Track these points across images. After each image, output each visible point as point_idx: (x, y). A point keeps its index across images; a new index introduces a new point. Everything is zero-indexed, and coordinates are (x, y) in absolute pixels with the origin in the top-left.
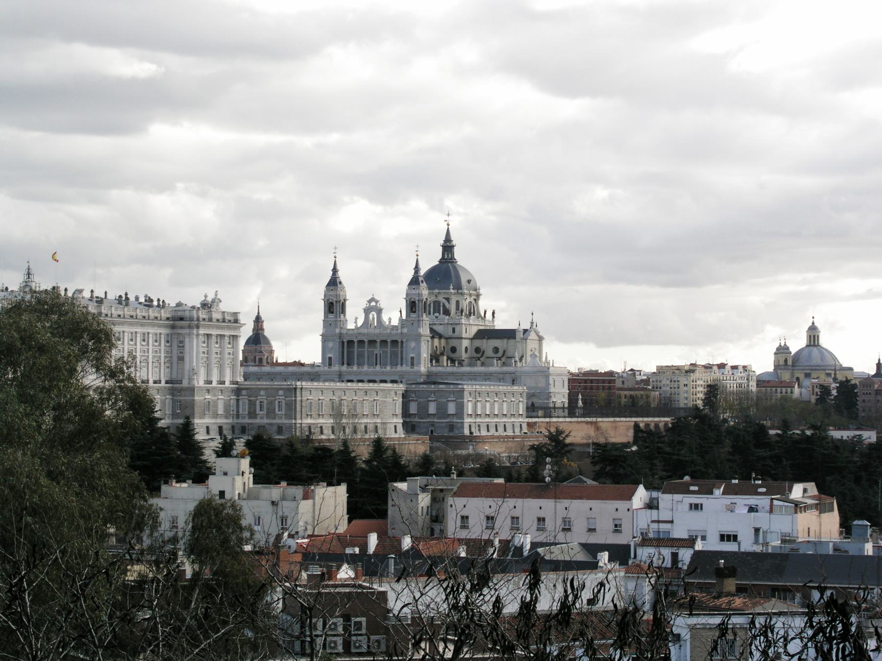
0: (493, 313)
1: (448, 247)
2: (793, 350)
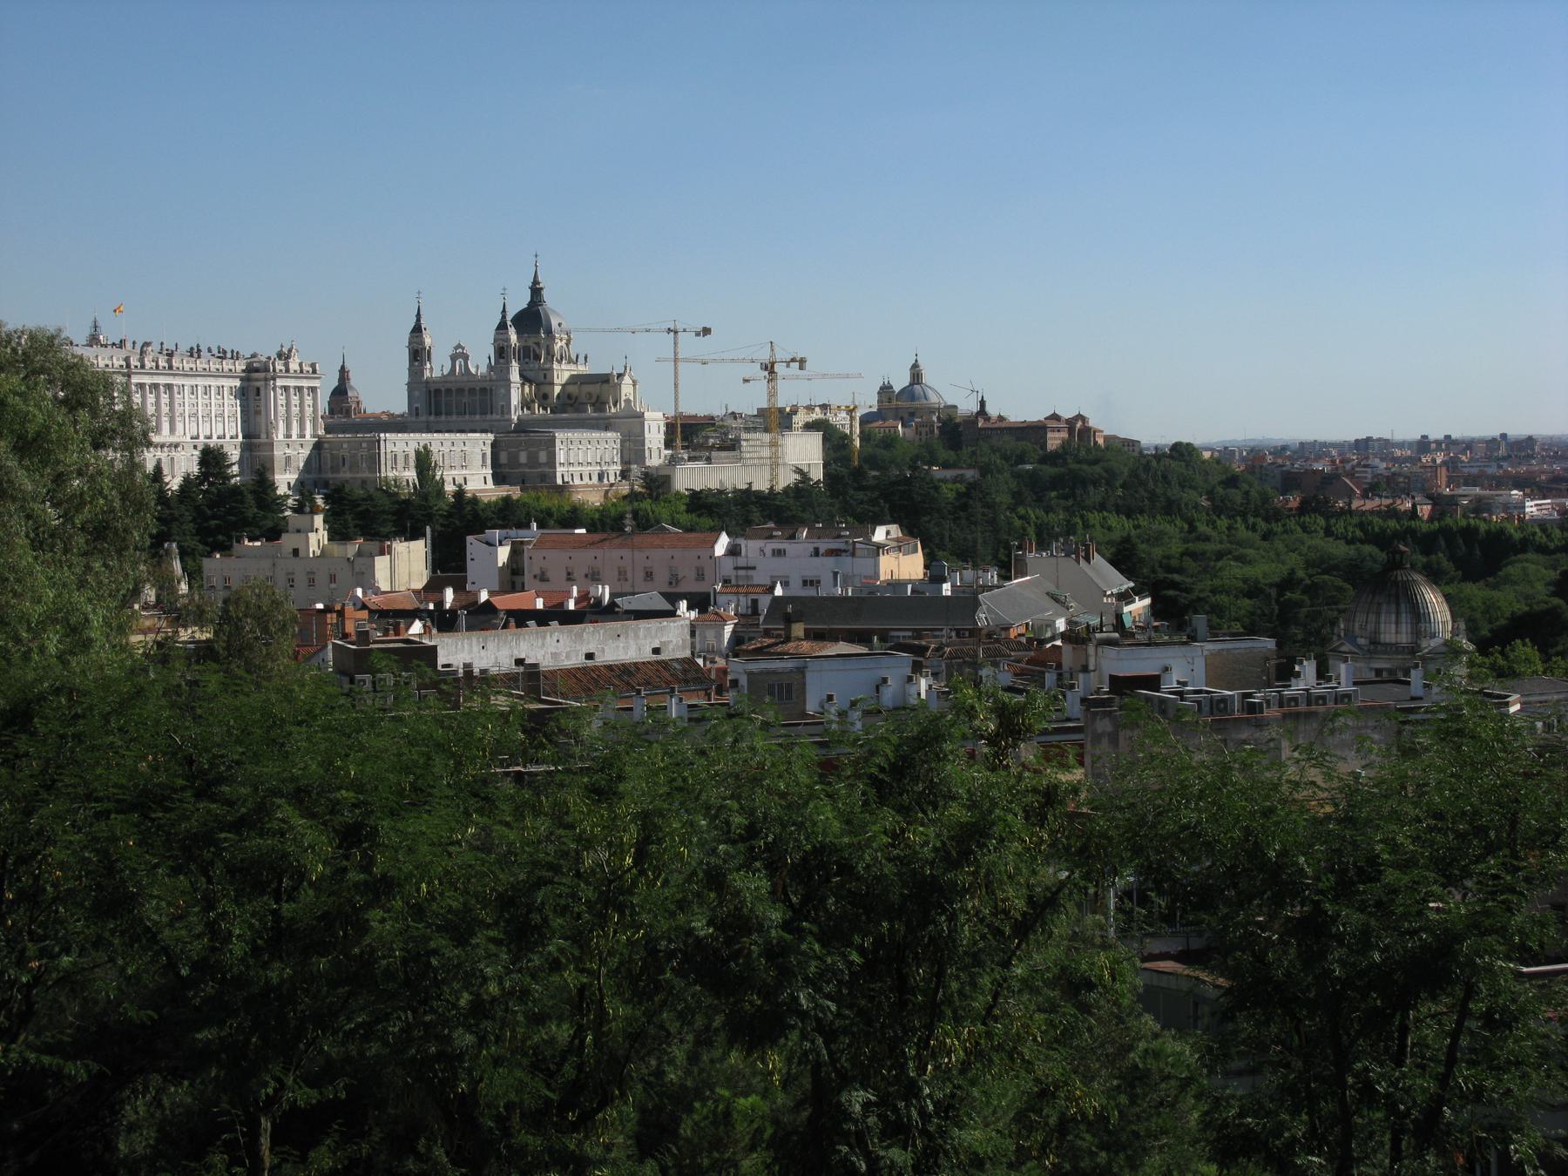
0: (586, 358)
1: (536, 291)
2: (897, 389)
